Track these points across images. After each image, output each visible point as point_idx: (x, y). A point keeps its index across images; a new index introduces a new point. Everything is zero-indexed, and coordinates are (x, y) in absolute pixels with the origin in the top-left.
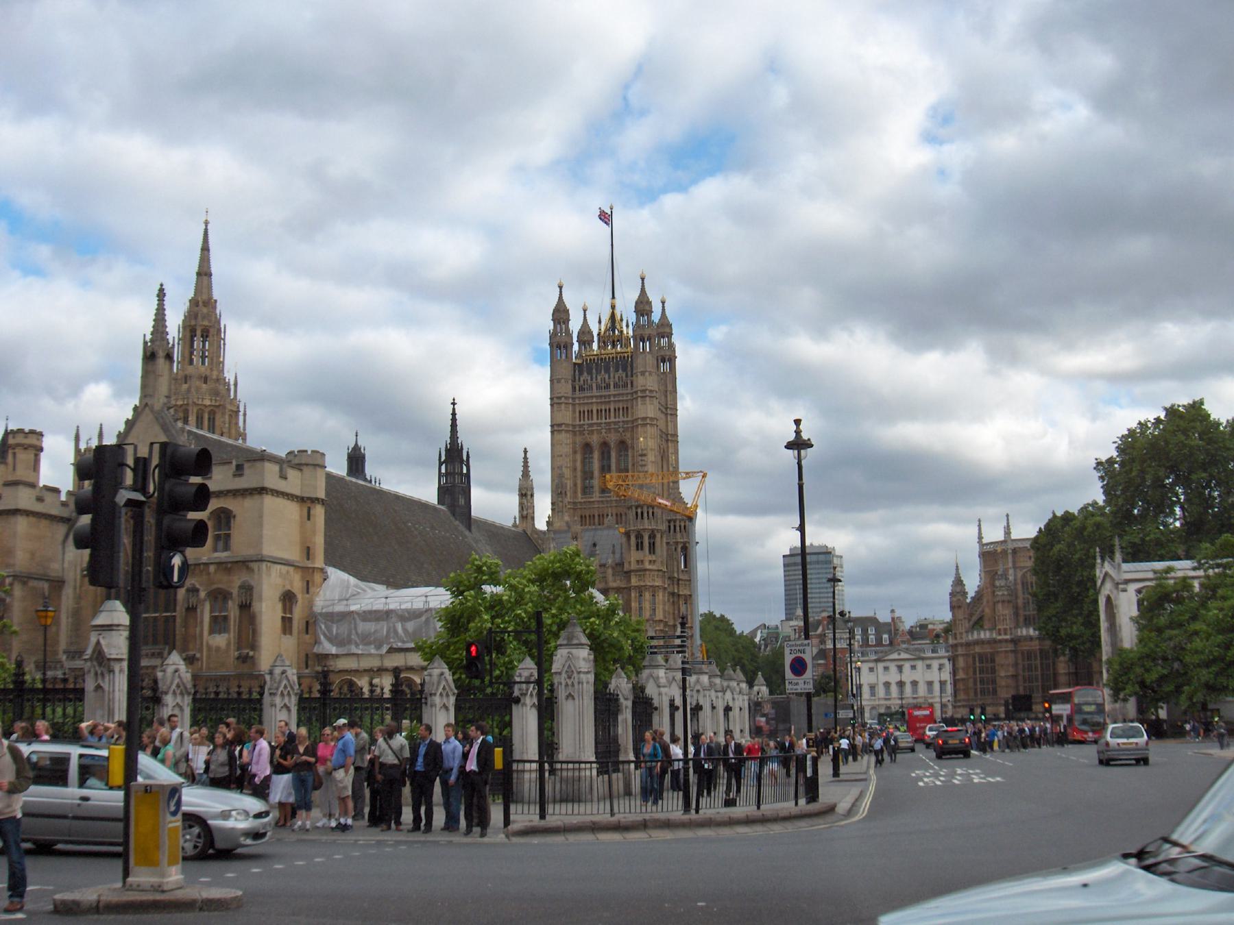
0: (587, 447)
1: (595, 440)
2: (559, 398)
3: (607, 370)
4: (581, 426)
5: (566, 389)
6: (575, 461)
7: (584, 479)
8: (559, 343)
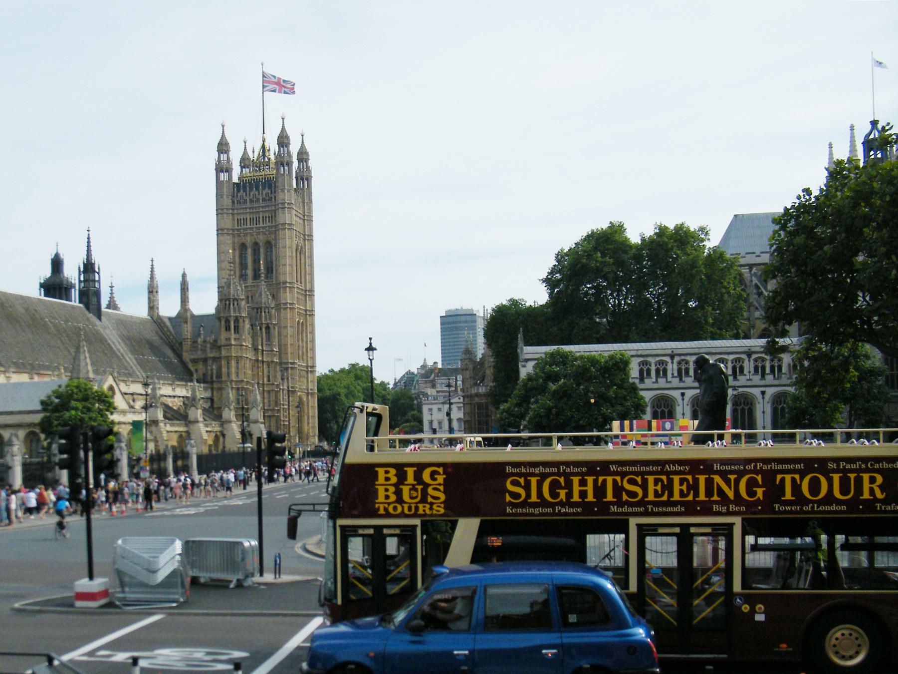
0: (243, 247)
1: (249, 240)
2: (222, 209)
3: (257, 189)
4: (238, 230)
5: (227, 202)
7: (241, 270)
8: (222, 168)
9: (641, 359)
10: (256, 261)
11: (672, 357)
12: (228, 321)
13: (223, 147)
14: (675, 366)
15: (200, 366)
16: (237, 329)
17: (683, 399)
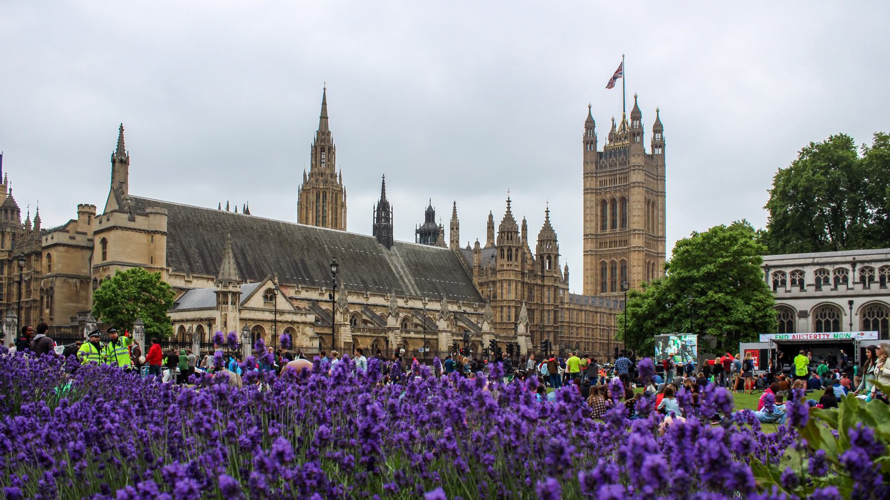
0: (604, 203)
3: (615, 156)
6: (597, 211)
8: (590, 141)
9: (818, 267)
10: (614, 214)
11: (854, 264)
12: (502, 250)
13: (590, 124)
14: (857, 275)
15: (485, 289)
16: (510, 258)
17: (851, 308)
